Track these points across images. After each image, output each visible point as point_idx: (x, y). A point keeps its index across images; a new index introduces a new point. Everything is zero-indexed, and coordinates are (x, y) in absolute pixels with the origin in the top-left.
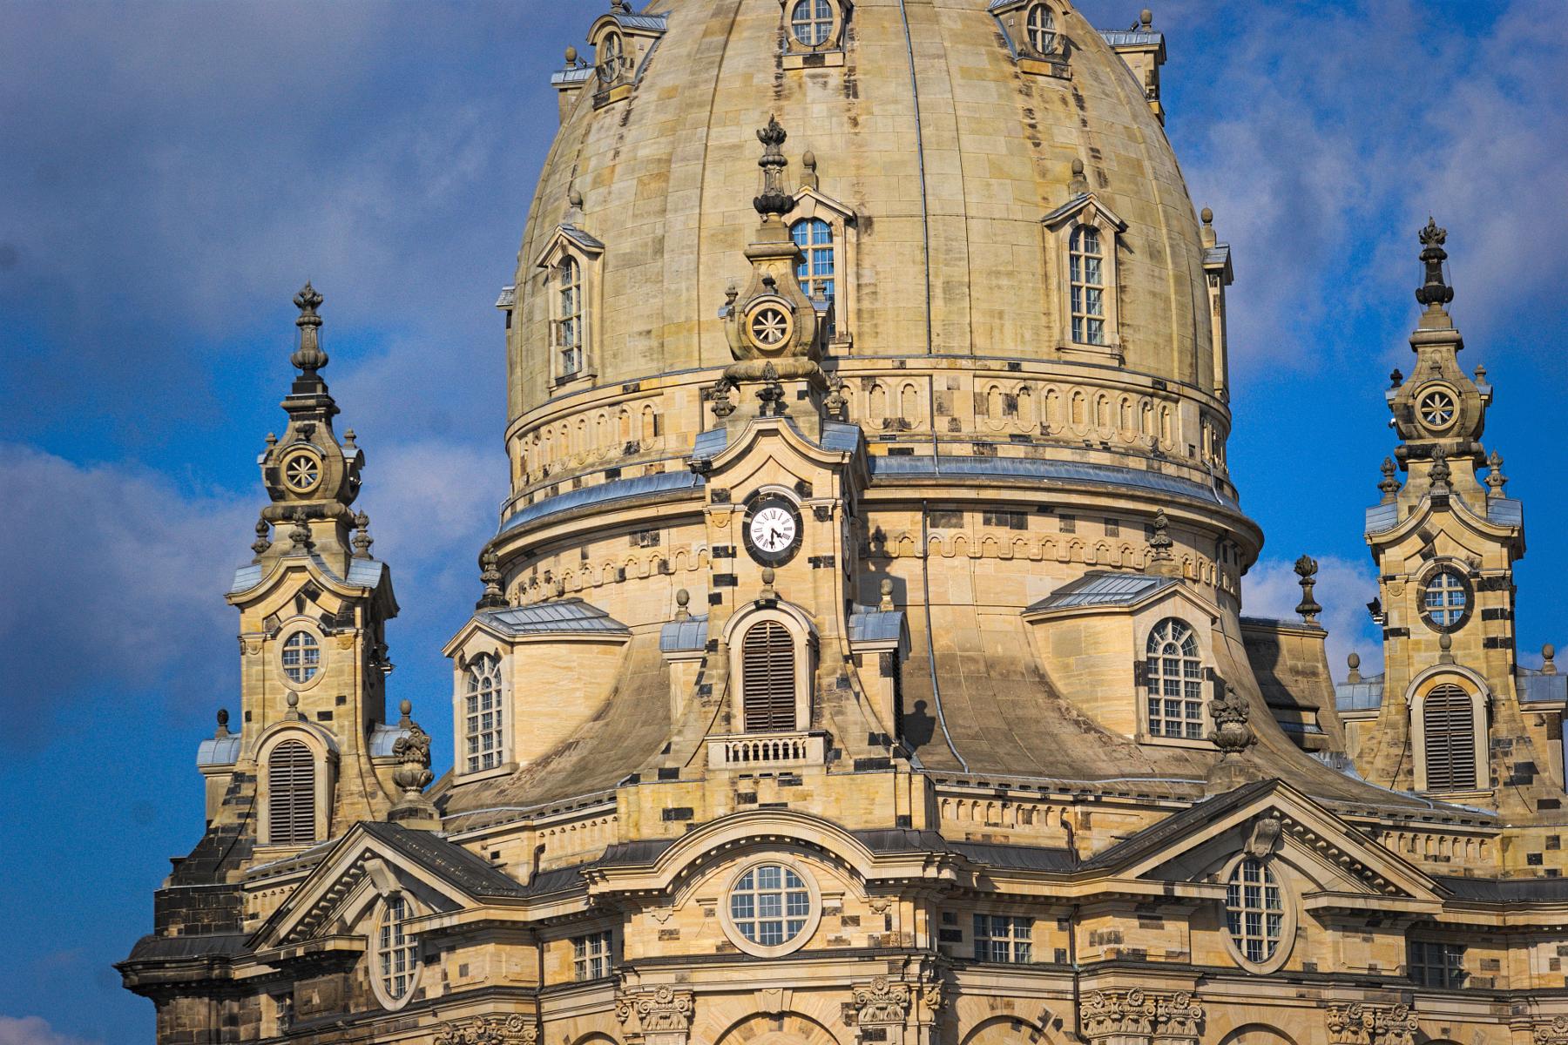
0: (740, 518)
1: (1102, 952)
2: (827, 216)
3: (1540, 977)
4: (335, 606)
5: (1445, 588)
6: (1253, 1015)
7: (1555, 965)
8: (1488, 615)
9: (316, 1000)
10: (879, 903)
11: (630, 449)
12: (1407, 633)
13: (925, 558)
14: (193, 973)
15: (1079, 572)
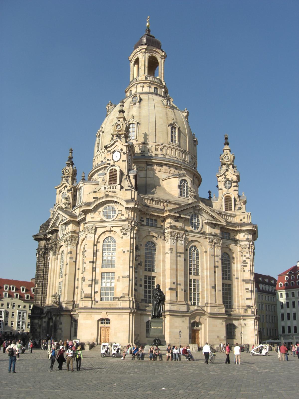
0: (111, 155)
1: (168, 225)
2: (134, 122)
3: (242, 238)
4: (69, 188)
5: (228, 183)
6: (194, 239)
7: (244, 236)
8: (234, 186)
9: (53, 238)
10: (128, 212)
11: (105, 158)
12: (222, 189)
13: (146, 171)
14: (42, 237)
15: (171, 175)
